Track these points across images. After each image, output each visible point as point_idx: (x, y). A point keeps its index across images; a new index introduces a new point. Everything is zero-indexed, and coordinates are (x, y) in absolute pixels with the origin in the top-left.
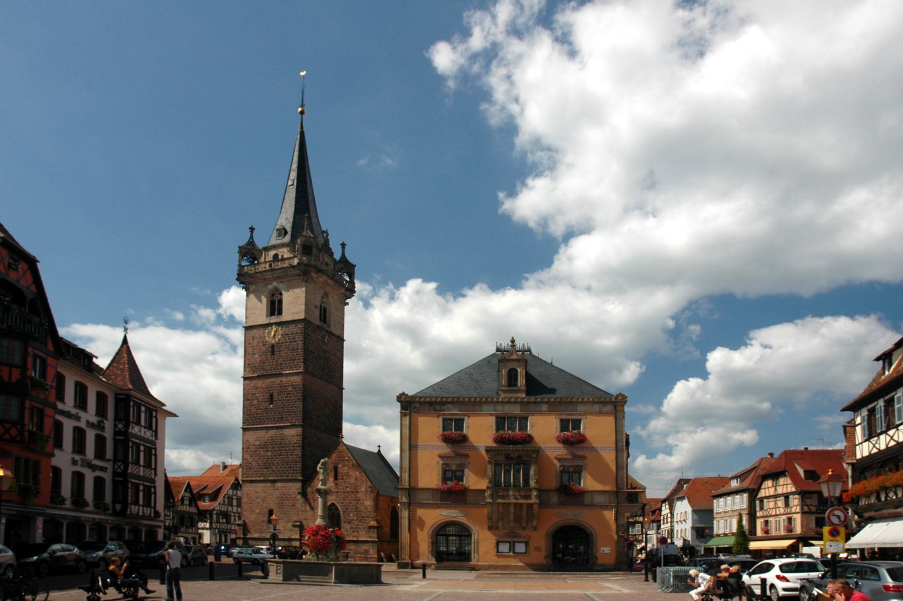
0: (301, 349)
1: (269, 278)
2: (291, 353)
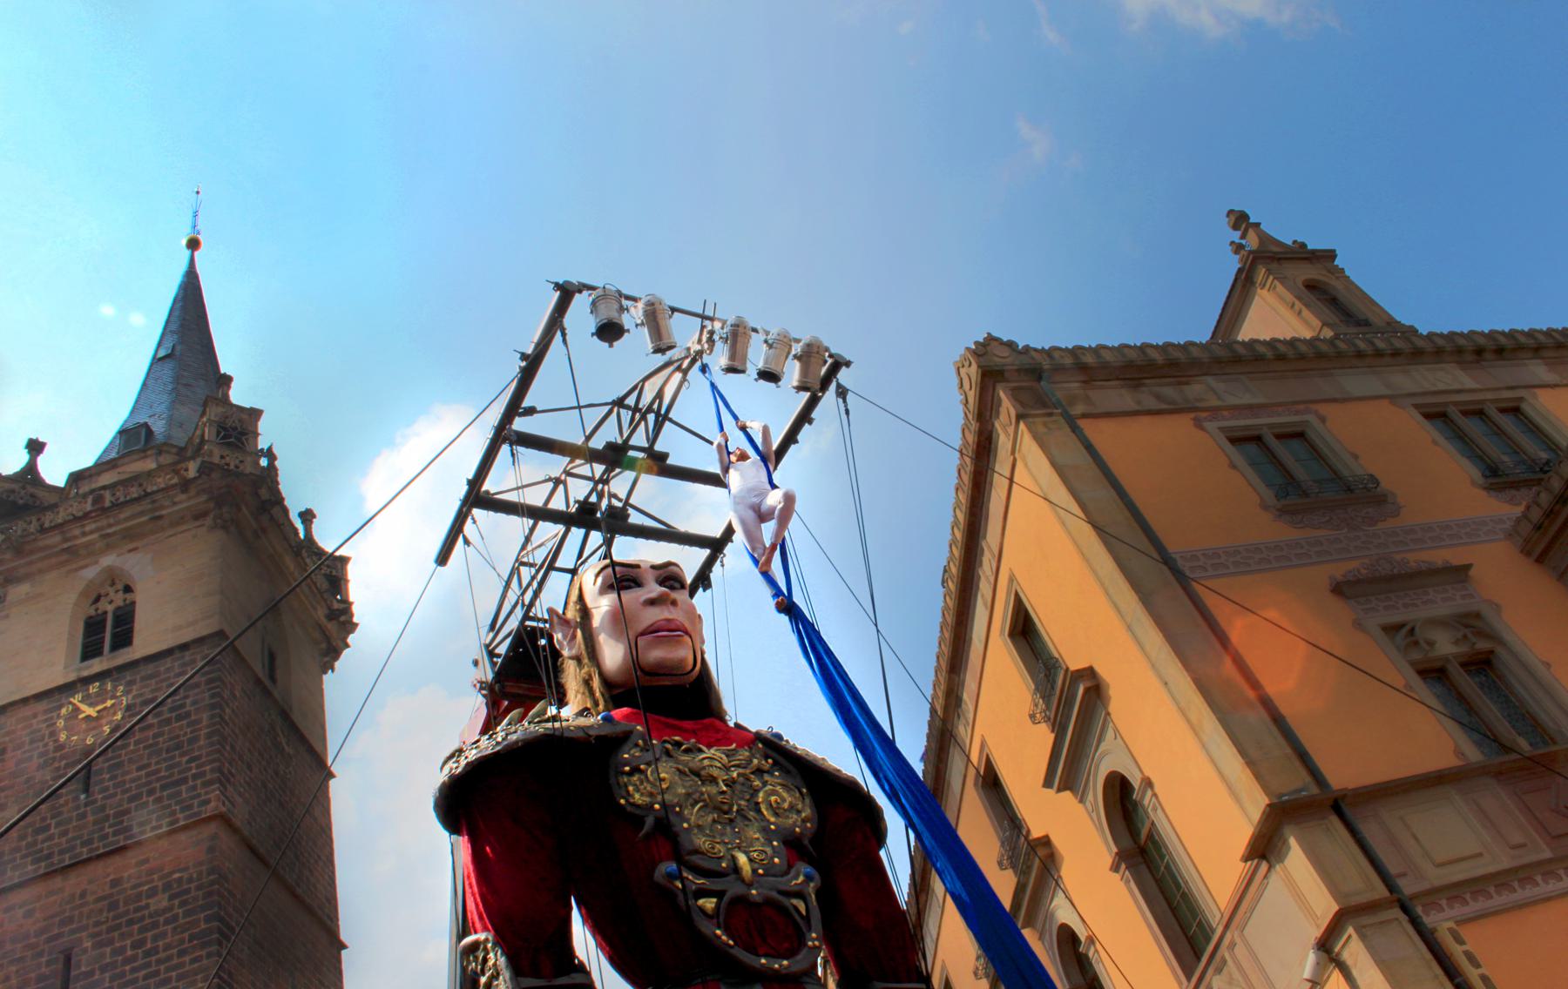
0: (209, 736)
1: (87, 545)
2: (165, 760)
